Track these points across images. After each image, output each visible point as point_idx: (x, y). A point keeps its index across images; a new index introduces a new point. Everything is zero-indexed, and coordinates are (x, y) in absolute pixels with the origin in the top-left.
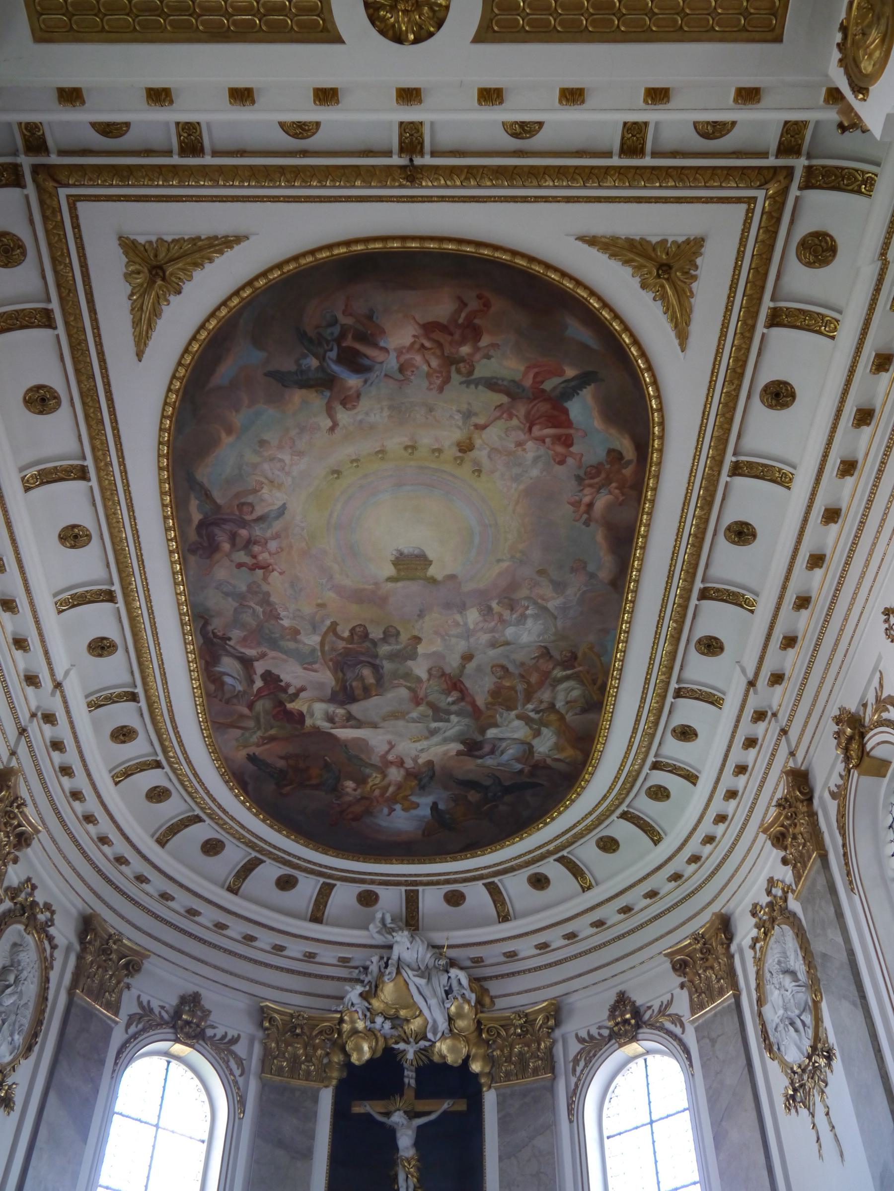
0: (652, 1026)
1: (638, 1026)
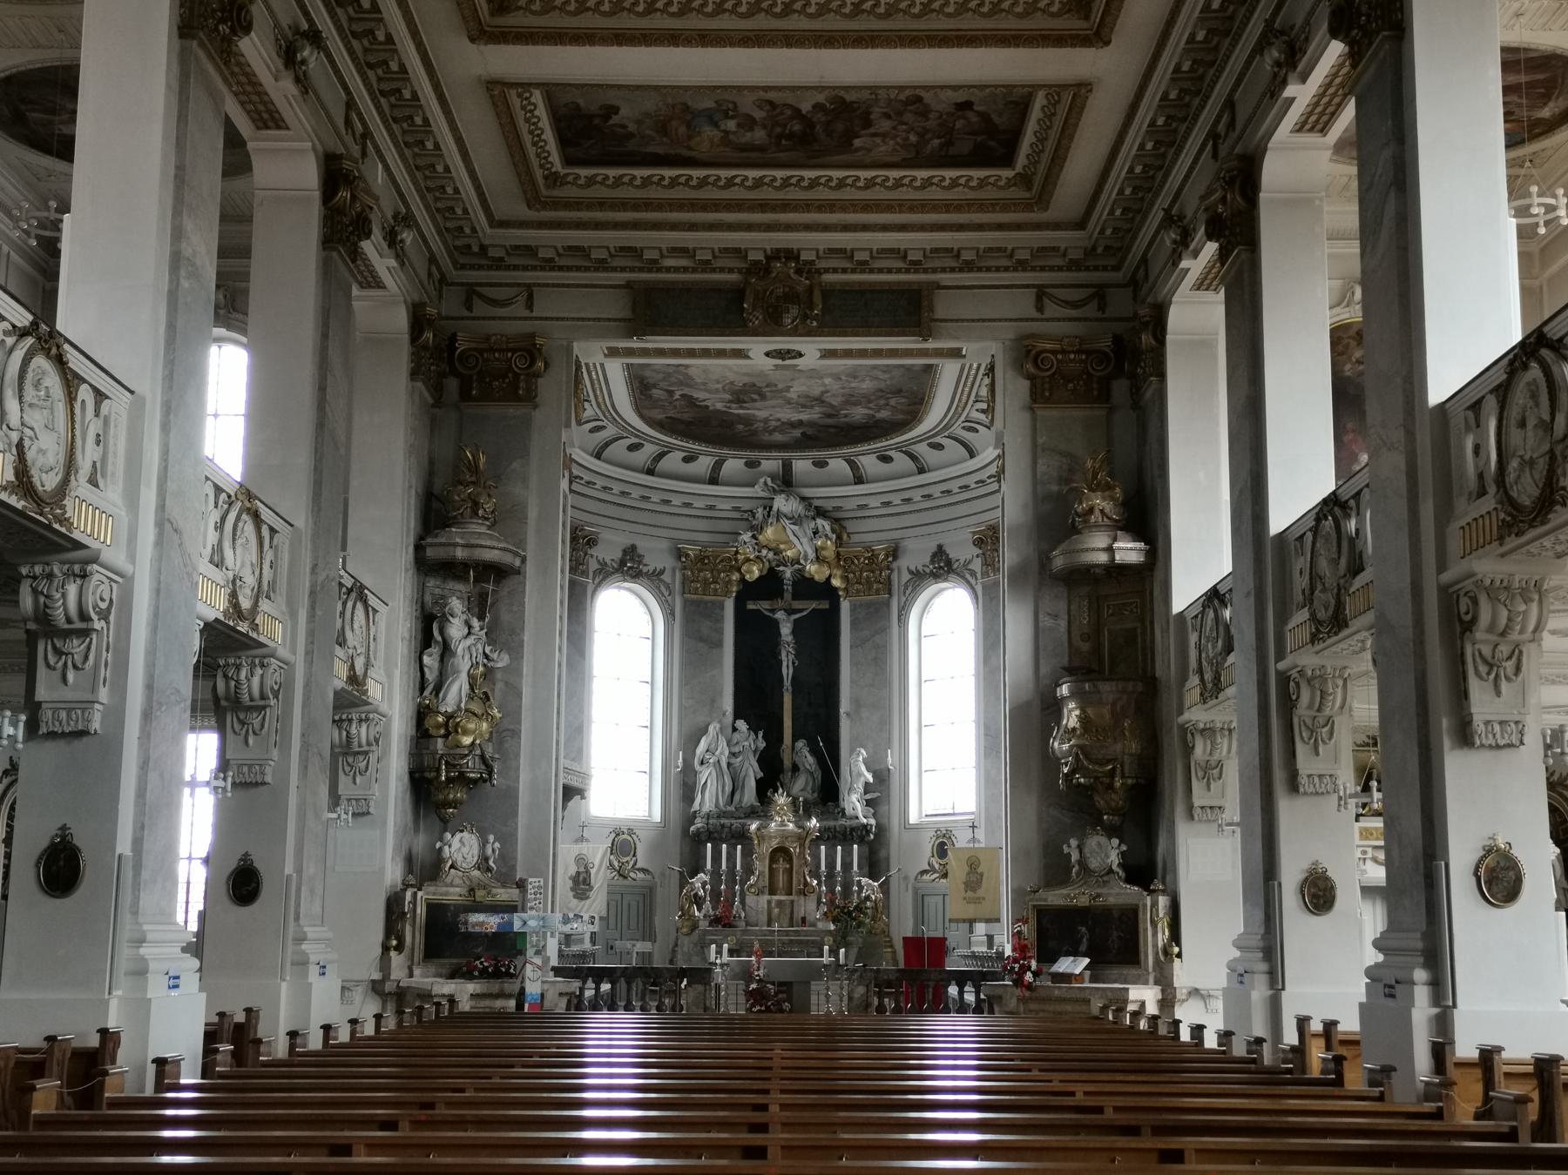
0: (958, 574)
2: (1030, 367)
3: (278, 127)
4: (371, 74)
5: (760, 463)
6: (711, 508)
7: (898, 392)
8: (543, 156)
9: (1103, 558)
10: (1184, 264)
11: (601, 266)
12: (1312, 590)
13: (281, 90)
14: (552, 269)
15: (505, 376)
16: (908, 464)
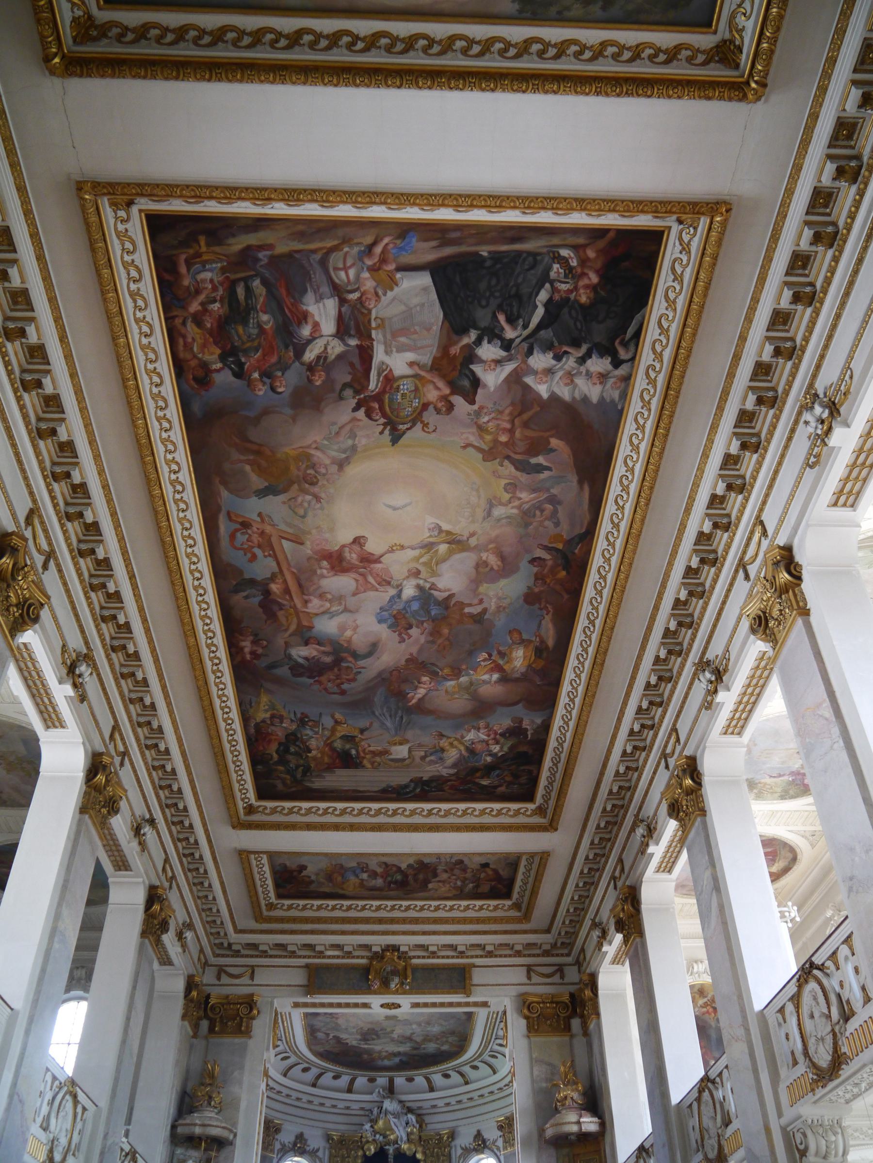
0: (489, 1149)
1: (484, 1148)
2: (526, 1011)
3: (126, 870)
4: (179, 844)
5: (376, 1080)
6: (348, 1108)
7: (453, 1033)
8: (266, 893)
9: (574, 1128)
10: (605, 949)
11: (293, 955)
12: (702, 1141)
13: (129, 846)
14: (266, 957)
15: (235, 1019)
16: (460, 1080)
